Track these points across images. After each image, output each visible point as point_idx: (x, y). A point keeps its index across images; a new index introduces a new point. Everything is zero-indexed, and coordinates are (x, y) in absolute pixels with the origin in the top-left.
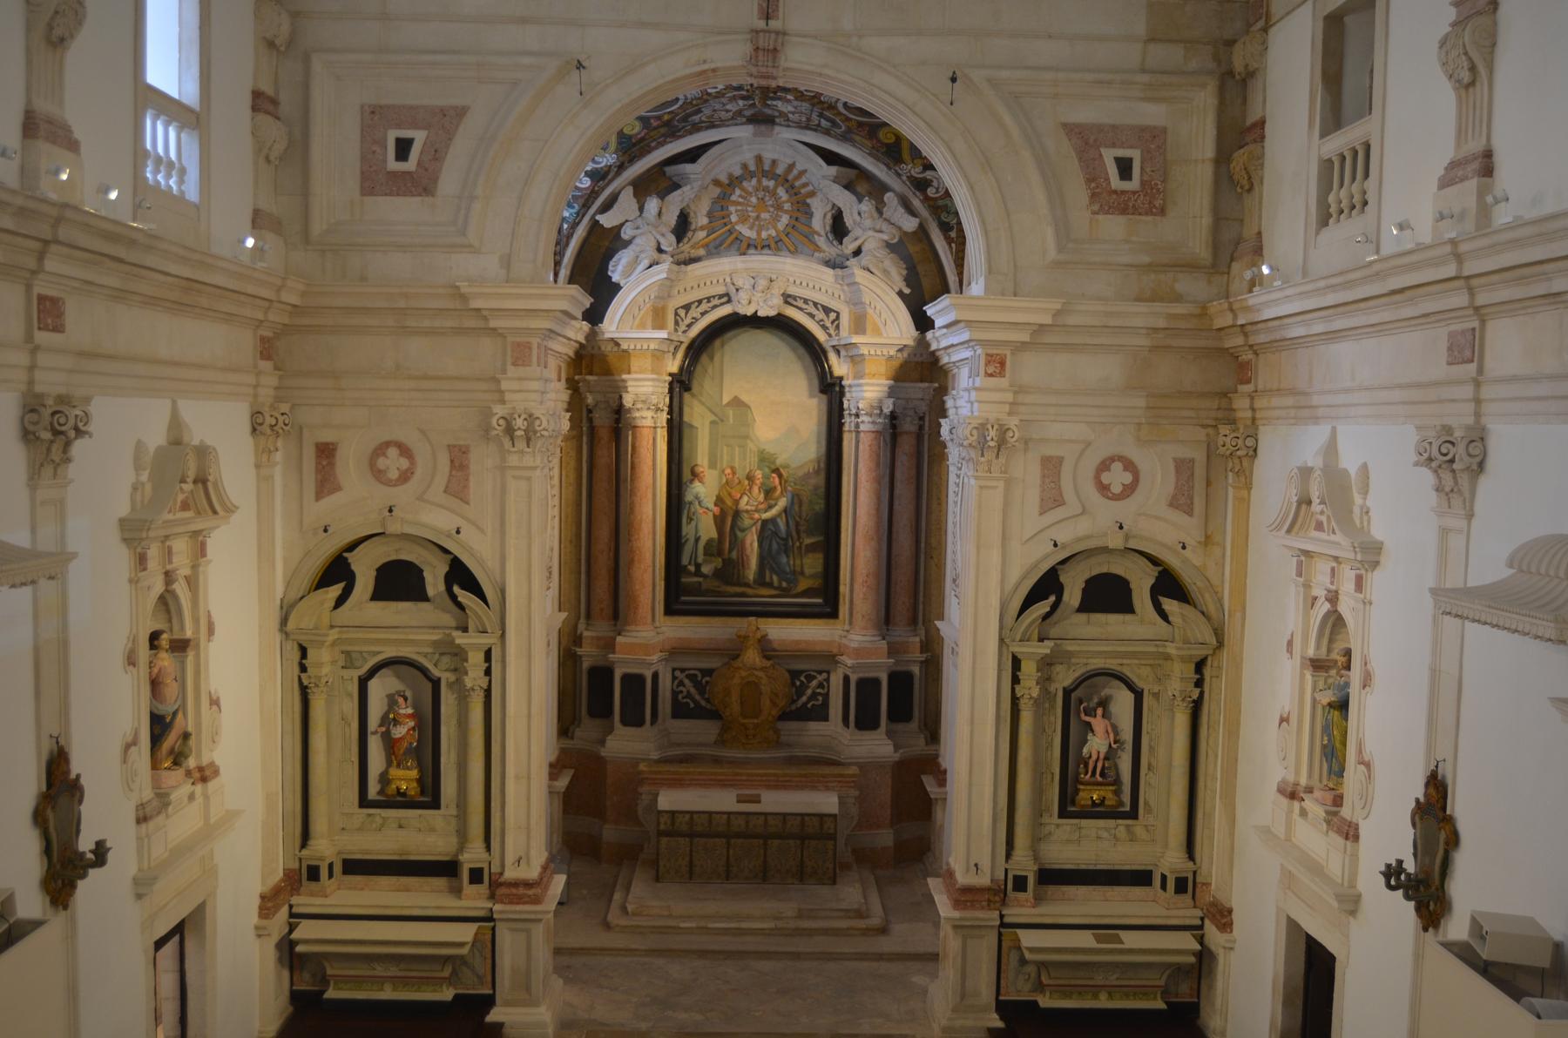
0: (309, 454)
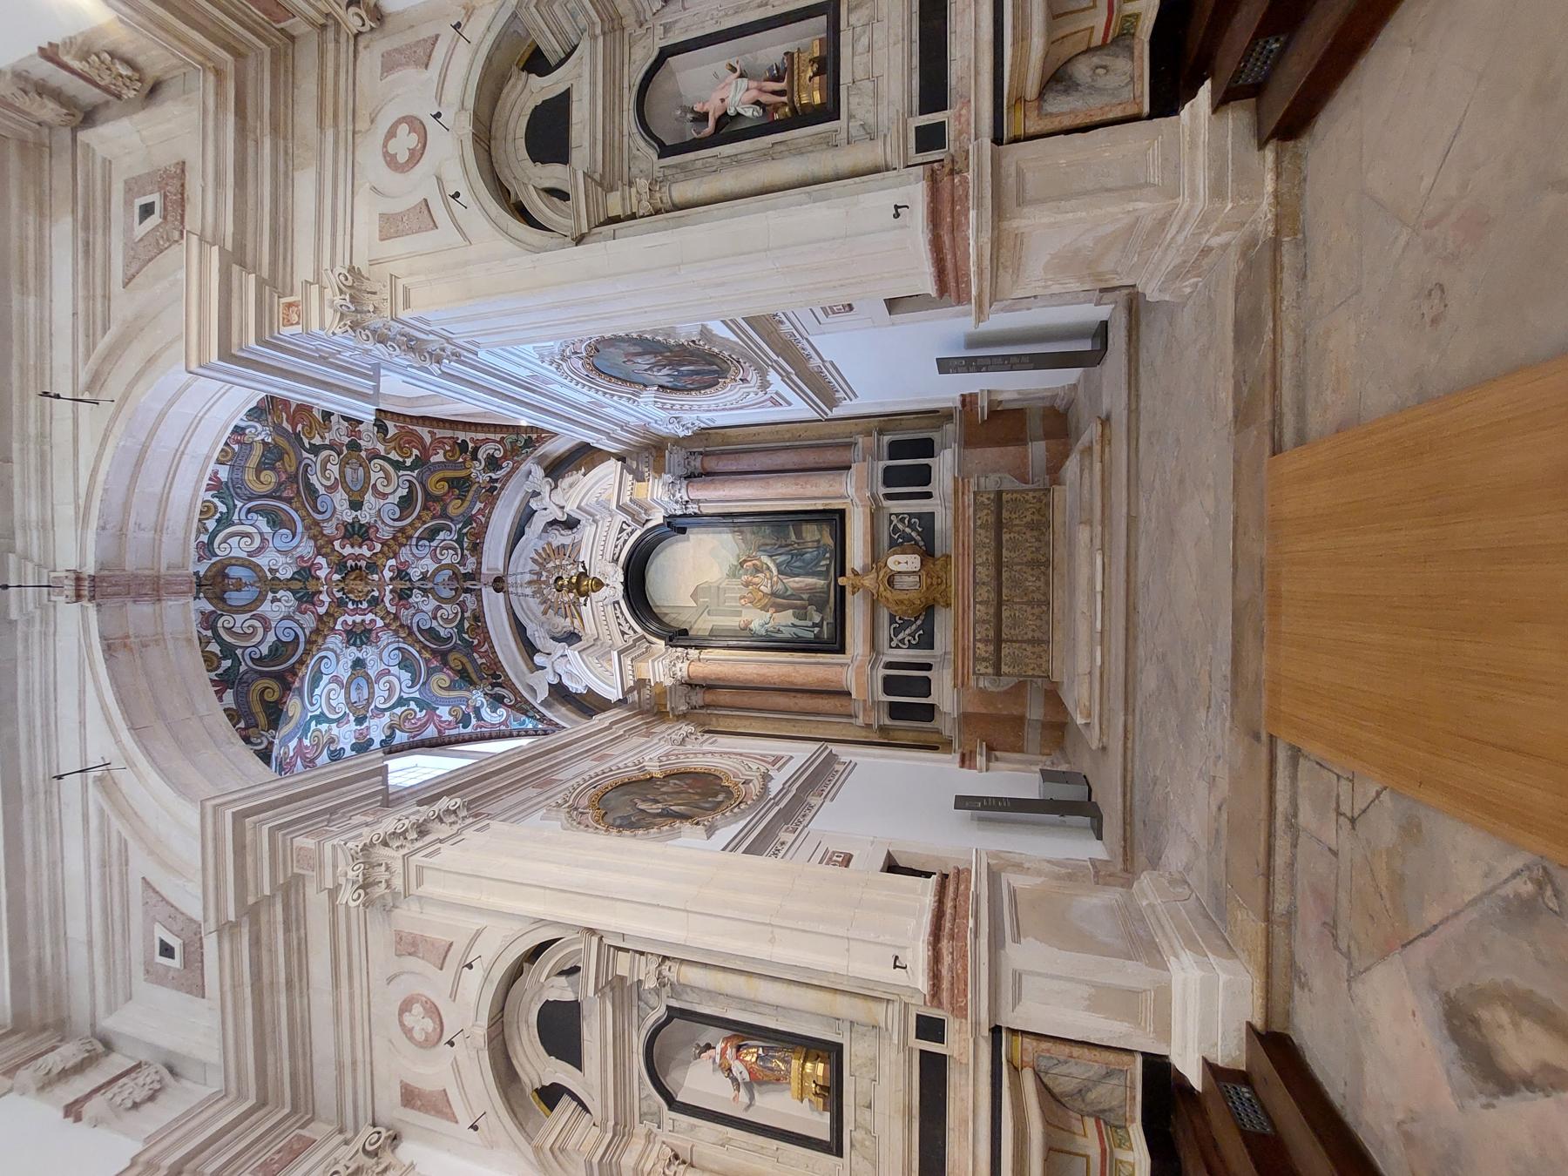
0: (411, 1116)
